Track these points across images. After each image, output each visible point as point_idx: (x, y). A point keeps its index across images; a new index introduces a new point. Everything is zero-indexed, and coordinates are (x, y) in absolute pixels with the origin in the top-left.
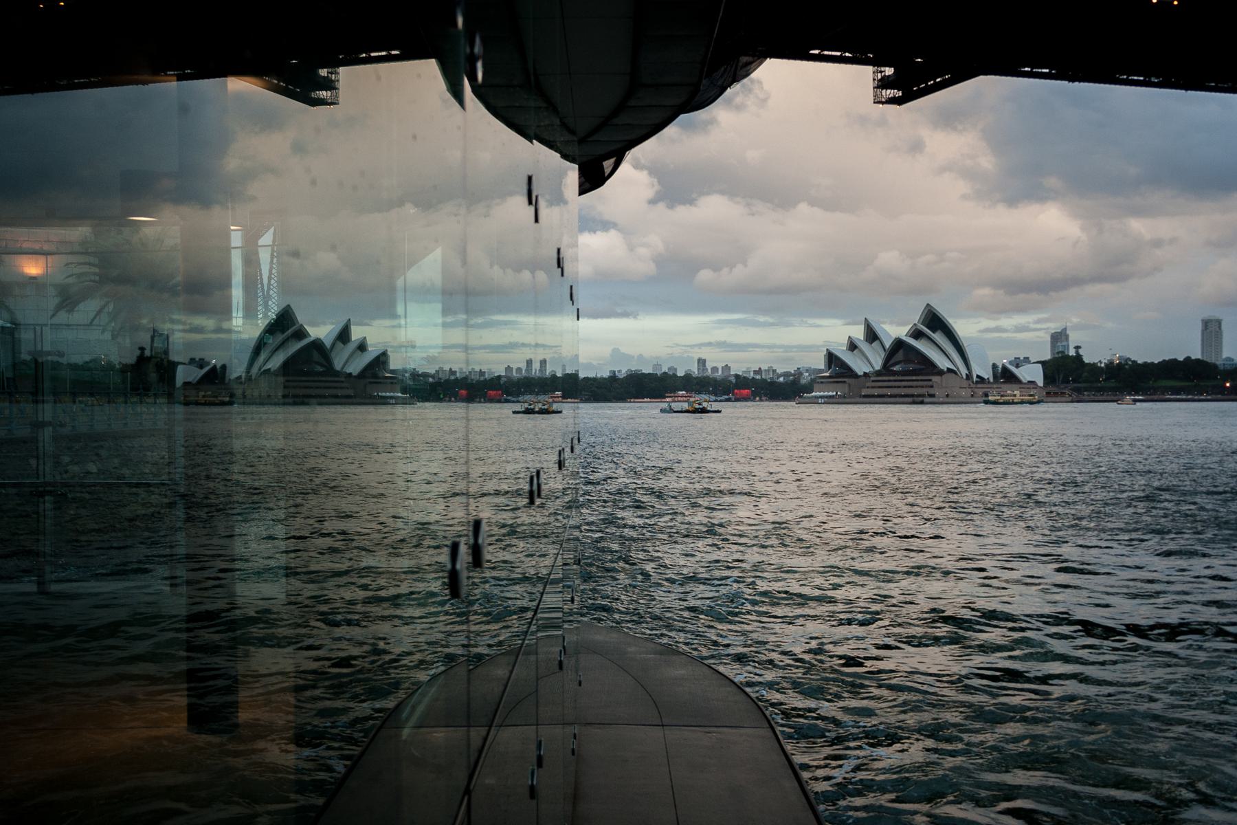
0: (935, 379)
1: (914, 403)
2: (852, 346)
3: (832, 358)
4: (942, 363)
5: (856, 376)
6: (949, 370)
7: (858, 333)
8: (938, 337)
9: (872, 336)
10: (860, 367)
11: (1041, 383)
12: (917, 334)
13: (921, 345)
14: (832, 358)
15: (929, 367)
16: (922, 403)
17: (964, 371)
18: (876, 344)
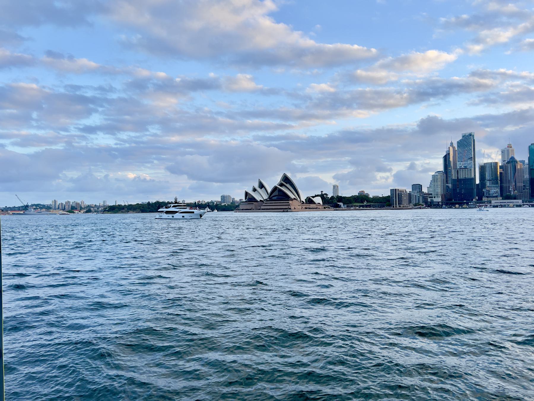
0: (290, 202)
1: (284, 211)
2: (255, 190)
3: (247, 194)
4: (292, 196)
5: (257, 201)
6: (295, 199)
7: (257, 186)
8: (288, 185)
9: (262, 186)
10: (258, 198)
11: (321, 203)
12: (281, 185)
13: (283, 189)
14: (247, 194)
15: (287, 198)
16: (287, 211)
17: (299, 200)
18: (263, 189)
